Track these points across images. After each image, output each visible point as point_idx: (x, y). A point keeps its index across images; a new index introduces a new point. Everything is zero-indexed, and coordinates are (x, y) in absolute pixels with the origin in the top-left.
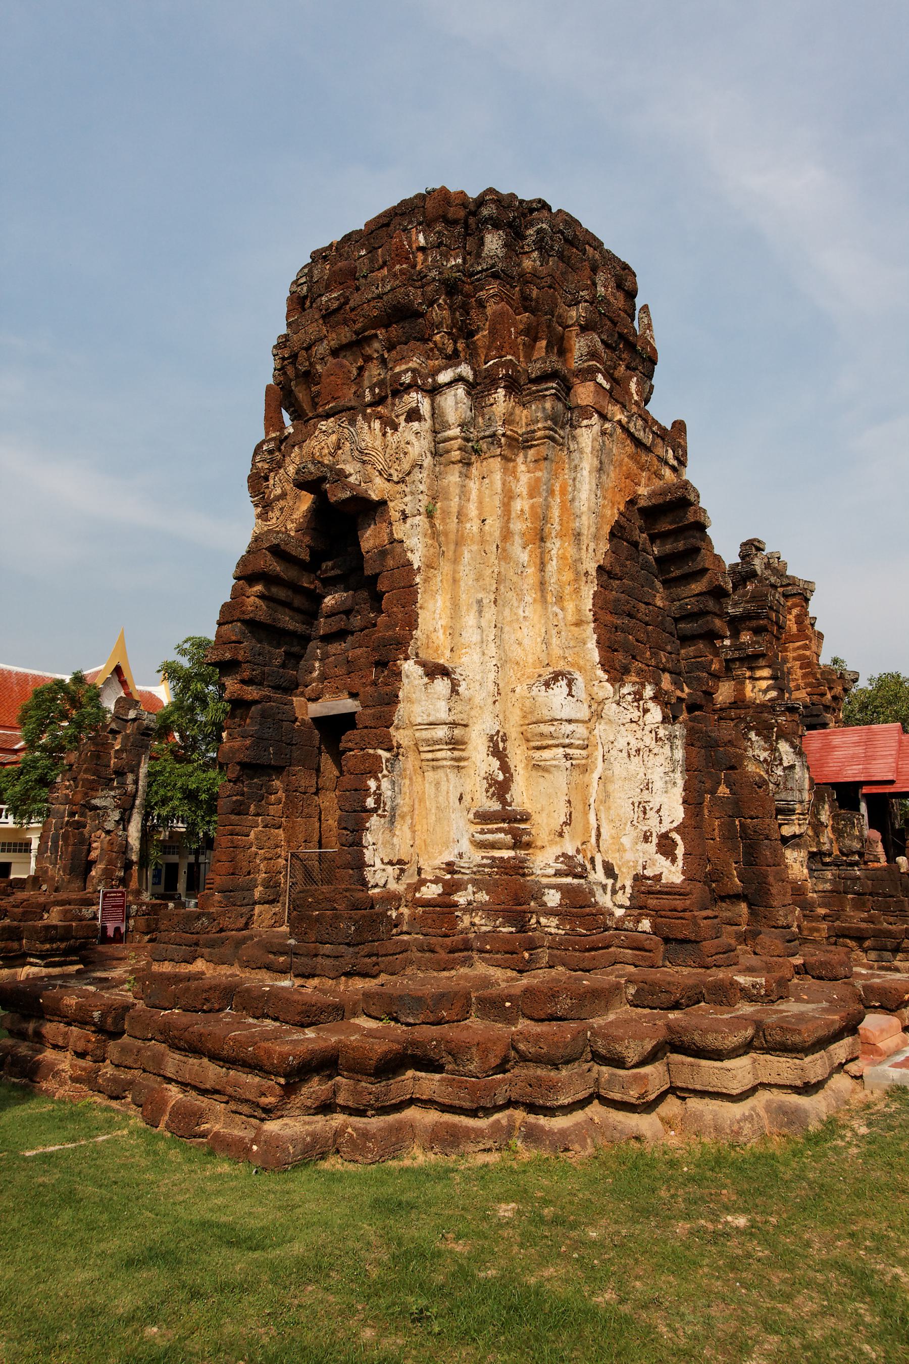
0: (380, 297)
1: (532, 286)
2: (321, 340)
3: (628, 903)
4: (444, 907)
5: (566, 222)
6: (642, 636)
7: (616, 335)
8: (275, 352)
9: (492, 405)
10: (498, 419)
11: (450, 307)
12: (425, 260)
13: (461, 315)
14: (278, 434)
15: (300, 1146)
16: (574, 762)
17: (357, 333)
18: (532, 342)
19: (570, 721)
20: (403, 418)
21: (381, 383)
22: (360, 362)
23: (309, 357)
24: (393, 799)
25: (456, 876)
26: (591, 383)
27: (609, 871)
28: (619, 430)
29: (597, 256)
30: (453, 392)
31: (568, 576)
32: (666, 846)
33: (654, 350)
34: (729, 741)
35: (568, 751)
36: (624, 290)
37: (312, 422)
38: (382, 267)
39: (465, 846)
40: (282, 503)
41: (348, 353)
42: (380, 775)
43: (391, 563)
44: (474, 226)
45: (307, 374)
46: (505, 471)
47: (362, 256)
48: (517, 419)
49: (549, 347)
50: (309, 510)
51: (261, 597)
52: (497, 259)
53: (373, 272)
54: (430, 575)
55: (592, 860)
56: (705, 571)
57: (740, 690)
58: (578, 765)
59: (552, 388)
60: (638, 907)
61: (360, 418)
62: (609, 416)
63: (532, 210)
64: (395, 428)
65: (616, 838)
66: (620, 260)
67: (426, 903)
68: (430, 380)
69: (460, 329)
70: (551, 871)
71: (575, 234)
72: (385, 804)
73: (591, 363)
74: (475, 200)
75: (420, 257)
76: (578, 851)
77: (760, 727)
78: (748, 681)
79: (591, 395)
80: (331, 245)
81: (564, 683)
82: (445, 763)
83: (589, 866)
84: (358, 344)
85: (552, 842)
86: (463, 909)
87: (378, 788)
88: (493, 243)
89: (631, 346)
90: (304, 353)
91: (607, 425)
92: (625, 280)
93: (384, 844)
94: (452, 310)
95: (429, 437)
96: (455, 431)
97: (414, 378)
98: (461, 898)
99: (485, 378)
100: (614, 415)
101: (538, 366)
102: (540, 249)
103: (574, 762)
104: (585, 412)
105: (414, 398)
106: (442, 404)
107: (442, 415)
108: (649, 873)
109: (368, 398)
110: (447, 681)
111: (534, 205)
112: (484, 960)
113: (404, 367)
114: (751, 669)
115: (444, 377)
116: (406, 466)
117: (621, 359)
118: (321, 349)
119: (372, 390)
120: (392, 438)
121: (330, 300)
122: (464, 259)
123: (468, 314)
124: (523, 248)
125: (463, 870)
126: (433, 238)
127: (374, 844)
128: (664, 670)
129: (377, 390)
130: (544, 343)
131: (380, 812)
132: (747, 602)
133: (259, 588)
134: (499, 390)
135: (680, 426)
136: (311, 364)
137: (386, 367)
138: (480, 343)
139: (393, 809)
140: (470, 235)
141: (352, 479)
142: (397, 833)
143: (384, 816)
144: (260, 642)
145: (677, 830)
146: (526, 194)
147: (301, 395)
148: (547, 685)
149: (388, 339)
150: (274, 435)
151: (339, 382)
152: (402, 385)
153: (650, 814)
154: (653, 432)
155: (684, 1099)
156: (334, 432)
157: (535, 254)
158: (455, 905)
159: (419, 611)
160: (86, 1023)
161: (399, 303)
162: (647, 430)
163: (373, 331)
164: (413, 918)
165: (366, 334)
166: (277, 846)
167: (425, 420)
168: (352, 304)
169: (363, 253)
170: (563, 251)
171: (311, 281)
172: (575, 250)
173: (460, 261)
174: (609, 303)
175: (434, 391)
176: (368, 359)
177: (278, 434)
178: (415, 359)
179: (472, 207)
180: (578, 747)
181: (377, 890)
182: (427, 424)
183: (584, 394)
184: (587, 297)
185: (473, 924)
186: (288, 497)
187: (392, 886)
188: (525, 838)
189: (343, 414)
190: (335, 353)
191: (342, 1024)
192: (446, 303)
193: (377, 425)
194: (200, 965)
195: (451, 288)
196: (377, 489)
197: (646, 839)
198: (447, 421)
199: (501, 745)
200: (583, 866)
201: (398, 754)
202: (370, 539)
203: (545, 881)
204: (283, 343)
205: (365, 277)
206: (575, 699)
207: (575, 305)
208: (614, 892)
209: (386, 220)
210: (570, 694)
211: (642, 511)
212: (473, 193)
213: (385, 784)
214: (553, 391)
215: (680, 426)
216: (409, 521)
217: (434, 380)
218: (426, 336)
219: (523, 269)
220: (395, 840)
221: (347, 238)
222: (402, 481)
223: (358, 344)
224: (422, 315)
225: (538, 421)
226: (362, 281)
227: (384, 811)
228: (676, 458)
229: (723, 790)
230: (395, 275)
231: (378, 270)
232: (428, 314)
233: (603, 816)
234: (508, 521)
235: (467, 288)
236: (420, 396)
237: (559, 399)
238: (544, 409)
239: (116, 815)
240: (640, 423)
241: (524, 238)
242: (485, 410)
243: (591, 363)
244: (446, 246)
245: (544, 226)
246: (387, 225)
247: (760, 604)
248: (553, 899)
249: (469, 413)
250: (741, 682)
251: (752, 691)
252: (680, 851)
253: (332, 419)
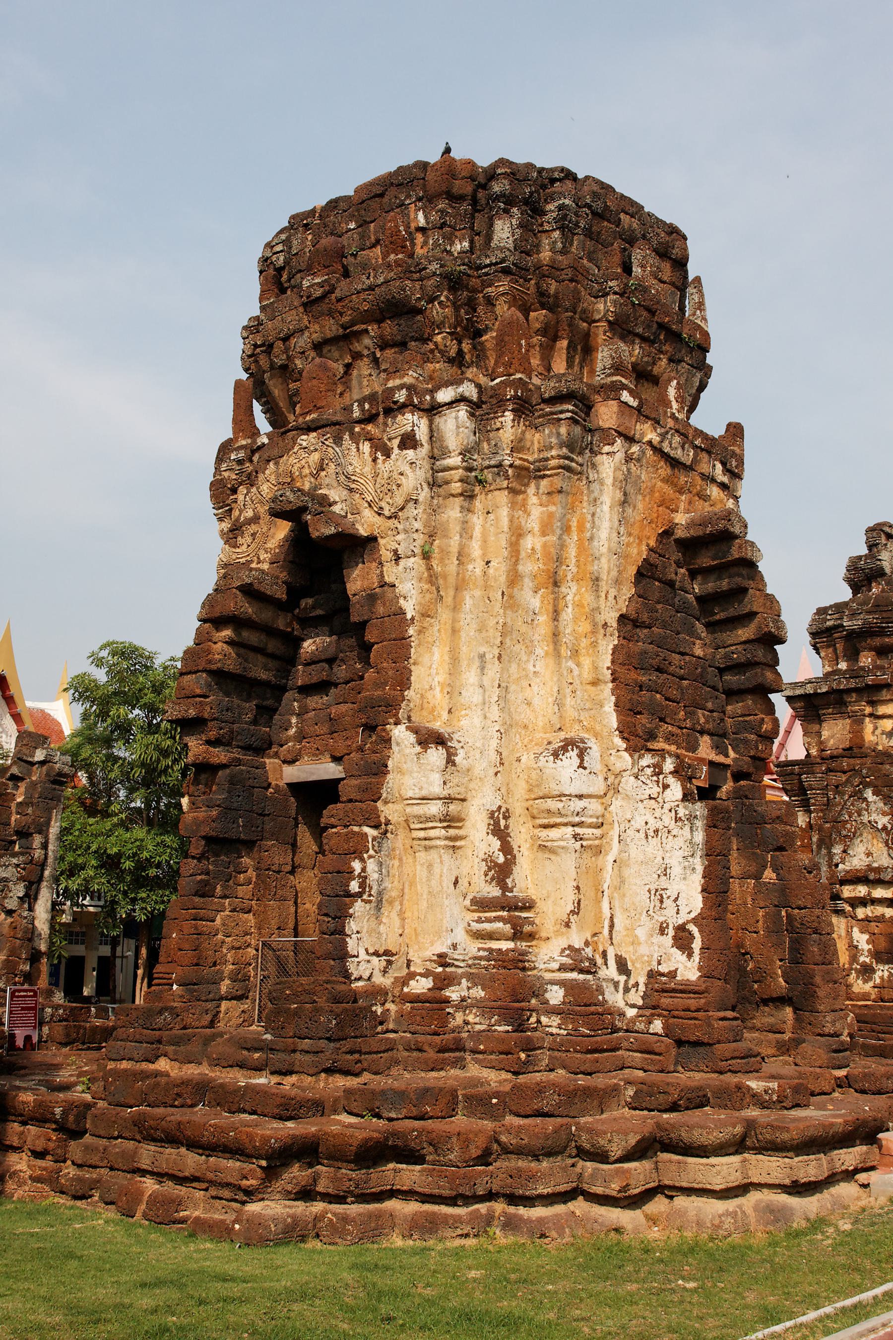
0: (371, 288)
1: (549, 281)
2: (302, 331)
3: (640, 1002)
4: (435, 1002)
5: (595, 195)
6: (674, 693)
7: (655, 326)
8: (245, 335)
9: (498, 429)
10: (505, 446)
11: (454, 304)
12: (426, 243)
13: (467, 313)
14: (249, 441)
15: (280, 1226)
16: (585, 843)
17: (344, 327)
18: (551, 343)
19: (580, 797)
20: (396, 442)
21: (372, 398)
22: (348, 360)
23: (286, 351)
24: (380, 882)
25: (448, 969)
26: (614, 403)
27: (623, 967)
28: (649, 452)
29: (635, 225)
30: (454, 414)
31: (585, 627)
32: (682, 940)
33: (706, 335)
34: (778, 817)
35: (578, 830)
36: (671, 259)
37: (291, 434)
38: (374, 246)
39: (460, 936)
40: (253, 528)
41: (333, 348)
42: (365, 856)
43: (381, 610)
44: (483, 201)
45: (284, 368)
46: (513, 505)
47: (350, 230)
48: (528, 444)
49: (571, 347)
50: (286, 539)
51: (230, 643)
52: (507, 253)
53: (363, 250)
54: (425, 625)
55: (604, 954)
56: (751, 615)
57: (857, 733)
58: (590, 847)
59: (568, 411)
60: (651, 1007)
61: (346, 436)
62: (637, 436)
63: (553, 181)
64: (387, 454)
65: (630, 930)
66: (664, 223)
67: (416, 999)
68: (428, 398)
69: (465, 329)
70: (556, 966)
71: (606, 205)
72: (371, 888)
73: (615, 378)
74: (485, 170)
75: (419, 238)
76: (587, 944)
77: (879, 783)
78: (867, 720)
79: (614, 416)
80: (314, 211)
81: (573, 754)
82: (438, 842)
83: (599, 961)
84: (346, 337)
85: (557, 933)
86: (456, 1006)
87: (364, 870)
88: (504, 232)
89: (675, 337)
90: (280, 344)
91: (635, 449)
92: (670, 247)
93: (369, 932)
94: (457, 308)
95: (426, 465)
96: (455, 460)
97: (409, 397)
98: (453, 994)
99: (491, 397)
100: (643, 435)
101: (552, 385)
102: (562, 228)
103: (585, 843)
104: (607, 436)
105: (409, 421)
106: (442, 426)
107: (441, 439)
108: (663, 969)
109: (356, 414)
110: (442, 751)
111: (556, 175)
112: (477, 1061)
113: (398, 382)
114: (872, 703)
115: (444, 395)
116: (399, 500)
117: (662, 352)
118: (301, 342)
119: (361, 405)
120: (384, 466)
121: (312, 286)
122: (472, 242)
123: (475, 311)
124: (542, 225)
125: (456, 963)
126: (434, 217)
127: (358, 932)
128: (702, 732)
129: (367, 406)
130: (565, 343)
131: (365, 897)
132: (869, 612)
133: (227, 633)
134: (507, 413)
135: (735, 431)
136: (289, 358)
137: (378, 368)
138: (488, 345)
139: (380, 893)
140: (479, 211)
141: (337, 509)
142: (384, 920)
143: (370, 902)
144: (227, 694)
145: (694, 921)
146: (546, 160)
147: (277, 390)
148: (556, 755)
149: (381, 337)
150: (244, 442)
151: (323, 388)
152: (395, 403)
153: (668, 903)
154: (695, 447)
155: (671, 1198)
156: (316, 450)
157: (556, 234)
158: (447, 1001)
159: (413, 668)
160: (46, 1121)
161: (394, 297)
162: (686, 446)
163: (364, 327)
164: (401, 1015)
165: (355, 328)
166: (246, 934)
167: (422, 445)
168: (338, 293)
169: (352, 226)
170: (591, 227)
171: (289, 253)
172: (606, 223)
173: (466, 244)
174: (645, 290)
175: (433, 410)
176: (357, 356)
177: (249, 441)
178: (411, 373)
179: (482, 179)
180: (590, 826)
181: (360, 984)
182: (424, 451)
183: (606, 414)
184: (616, 289)
185: (466, 1023)
186: (261, 521)
187: (378, 979)
188: (527, 928)
189: (328, 429)
190: (318, 347)
191: (324, 1119)
192: (448, 298)
193: (366, 447)
194: (163, 1064)
195: (454, 282)
196: (366, 523)
197: (662, 931)
198: (447, 447)
199: (502, 823)
200: (593, 962)
201: (386, 832)
202: (358, 580)
203: (548, 976)
204: (253, 328)
205: (355, 256)
206: (588, 771)
207: (602, 296)
208: (627, 990)
209: (378, 190)
210: (581, 766)
211: (680, 542)
212: (484, 161)
213: (371, 865)
214: (569, 415)
215: (735, 431)
216: (402, 562)
217: (433, 398)
218: (426, 336)
219: (539, 260)
220: (382, 928)
221: (333, 204)
222: (394, 516)
223: (346, 337)
224: (420, 311)
225: (552, 448)
226: (351, 259)
227: (370, 895)
228: (727, 470)
229: (769, 875)
230: (389, 266)
231: (370, 248)
232: (428, 311)
233: (616, 904)
234: (516, 563)
235: (474, 282)
236: (416, 417)
237: (576, 422)
238: (558, 434)
239: (19, 890)
240: (677, 439)
241: (543, 213)
242: (491, 435)
243: (615, 378)
244: (450, 226)
245: (567, 202)
246: (381, 195)
247: (885, 615)
248: (555, 996)
249: (472, 438)
250: (858, 720)
251: (873, 733)
252: (697, 945)
253: (315, 434)
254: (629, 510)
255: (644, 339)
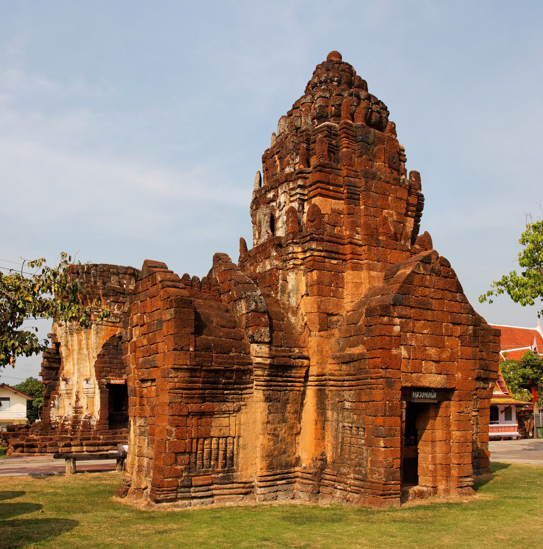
4: (63, 425)
46: (78, 336)
254: (99, 335)
255: (113, 296)
